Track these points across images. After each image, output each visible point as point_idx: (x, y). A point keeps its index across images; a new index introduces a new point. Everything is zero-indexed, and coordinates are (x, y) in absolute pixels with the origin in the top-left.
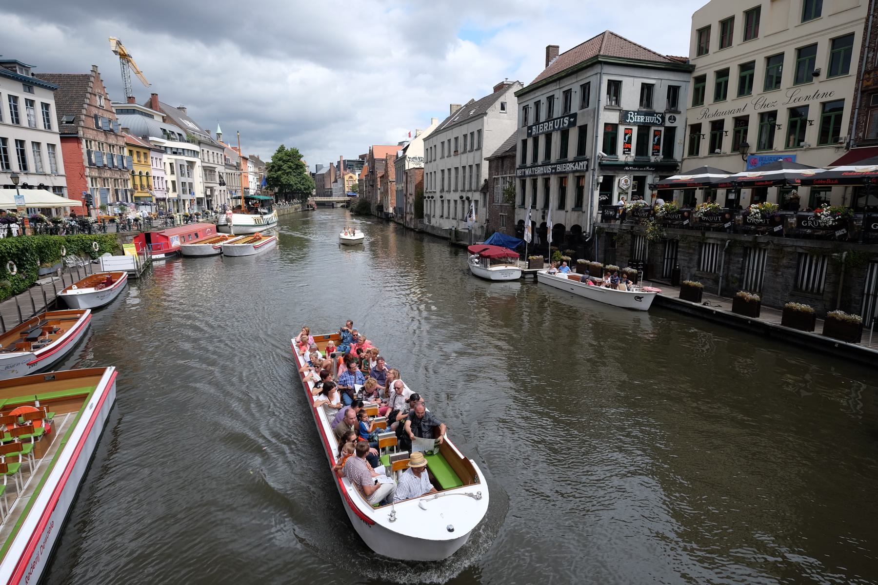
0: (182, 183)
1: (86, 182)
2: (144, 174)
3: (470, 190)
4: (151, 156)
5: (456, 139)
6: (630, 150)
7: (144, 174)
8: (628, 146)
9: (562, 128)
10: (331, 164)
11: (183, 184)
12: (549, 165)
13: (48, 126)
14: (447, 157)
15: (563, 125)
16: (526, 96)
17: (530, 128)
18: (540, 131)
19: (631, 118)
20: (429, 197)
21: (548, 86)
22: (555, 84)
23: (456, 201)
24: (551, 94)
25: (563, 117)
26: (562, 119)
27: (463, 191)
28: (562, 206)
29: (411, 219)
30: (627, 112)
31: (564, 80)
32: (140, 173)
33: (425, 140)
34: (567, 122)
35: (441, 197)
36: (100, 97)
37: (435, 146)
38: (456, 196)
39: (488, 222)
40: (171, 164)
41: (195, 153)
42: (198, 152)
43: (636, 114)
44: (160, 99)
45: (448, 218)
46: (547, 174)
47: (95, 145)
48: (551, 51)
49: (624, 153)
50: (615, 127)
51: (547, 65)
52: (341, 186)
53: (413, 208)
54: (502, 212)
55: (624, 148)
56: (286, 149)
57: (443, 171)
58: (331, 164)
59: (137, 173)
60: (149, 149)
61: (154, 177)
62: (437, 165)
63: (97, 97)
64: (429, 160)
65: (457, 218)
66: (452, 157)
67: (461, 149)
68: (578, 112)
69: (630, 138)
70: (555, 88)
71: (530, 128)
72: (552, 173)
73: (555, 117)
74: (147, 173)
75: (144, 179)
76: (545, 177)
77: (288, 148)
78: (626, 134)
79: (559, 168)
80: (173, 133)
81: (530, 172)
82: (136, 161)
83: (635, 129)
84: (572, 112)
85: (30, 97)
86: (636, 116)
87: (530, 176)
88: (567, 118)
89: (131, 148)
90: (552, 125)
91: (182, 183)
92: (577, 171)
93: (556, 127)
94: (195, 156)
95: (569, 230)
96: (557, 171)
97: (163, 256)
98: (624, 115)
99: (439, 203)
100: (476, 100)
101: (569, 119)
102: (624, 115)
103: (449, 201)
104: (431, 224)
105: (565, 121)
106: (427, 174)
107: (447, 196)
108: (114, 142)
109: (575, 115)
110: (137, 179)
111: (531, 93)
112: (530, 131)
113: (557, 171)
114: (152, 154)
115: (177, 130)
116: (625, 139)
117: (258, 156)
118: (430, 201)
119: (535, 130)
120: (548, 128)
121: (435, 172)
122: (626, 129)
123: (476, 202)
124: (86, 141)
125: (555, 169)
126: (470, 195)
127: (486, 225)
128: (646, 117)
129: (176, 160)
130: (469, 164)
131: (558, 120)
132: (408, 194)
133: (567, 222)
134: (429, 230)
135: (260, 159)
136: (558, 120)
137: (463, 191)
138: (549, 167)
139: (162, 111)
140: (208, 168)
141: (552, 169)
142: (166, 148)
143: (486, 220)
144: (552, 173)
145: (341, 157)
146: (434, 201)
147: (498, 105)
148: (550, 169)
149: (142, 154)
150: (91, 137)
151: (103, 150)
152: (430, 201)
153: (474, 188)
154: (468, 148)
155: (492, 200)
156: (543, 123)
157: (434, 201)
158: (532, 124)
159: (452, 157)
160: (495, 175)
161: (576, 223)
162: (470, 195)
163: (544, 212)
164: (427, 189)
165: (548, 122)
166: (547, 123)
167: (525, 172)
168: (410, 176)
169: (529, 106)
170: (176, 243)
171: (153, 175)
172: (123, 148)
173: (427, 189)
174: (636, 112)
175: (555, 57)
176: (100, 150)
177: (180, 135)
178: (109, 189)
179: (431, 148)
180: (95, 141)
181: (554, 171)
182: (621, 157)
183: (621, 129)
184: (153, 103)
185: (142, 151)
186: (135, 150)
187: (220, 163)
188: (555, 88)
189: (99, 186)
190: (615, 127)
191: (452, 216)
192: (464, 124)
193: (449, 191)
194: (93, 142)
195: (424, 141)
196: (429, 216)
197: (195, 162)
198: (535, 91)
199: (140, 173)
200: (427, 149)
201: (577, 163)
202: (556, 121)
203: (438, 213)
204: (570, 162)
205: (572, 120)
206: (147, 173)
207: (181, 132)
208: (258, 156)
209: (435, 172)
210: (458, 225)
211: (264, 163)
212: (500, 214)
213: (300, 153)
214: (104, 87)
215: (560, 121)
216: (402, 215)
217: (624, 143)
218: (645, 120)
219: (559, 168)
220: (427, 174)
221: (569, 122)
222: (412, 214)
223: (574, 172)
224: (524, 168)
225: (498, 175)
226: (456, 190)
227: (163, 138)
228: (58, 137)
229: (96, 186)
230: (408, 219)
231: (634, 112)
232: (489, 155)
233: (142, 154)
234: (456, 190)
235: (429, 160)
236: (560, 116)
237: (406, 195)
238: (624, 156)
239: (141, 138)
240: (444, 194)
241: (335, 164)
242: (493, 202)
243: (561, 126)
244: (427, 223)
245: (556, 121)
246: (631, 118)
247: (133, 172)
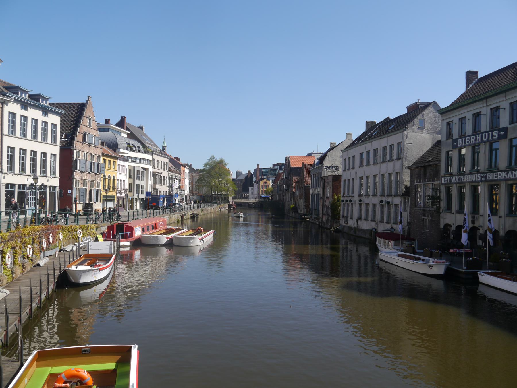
0: (137, 185)
1: (72, 183)
2: (112, 177)
3: (390, 195)
4: (118, 163)
5: (376, 151)
7: (112, 177)
9: (491, 141)
10: (249, 171)
11: (138, 186)
12: (478, 174)
13: (54, 141)
14: (366, 166)
15: (492, 137)
16: (450, 113)
17: (456, 141)
18: (467, 143)
20: (347, 201)
21: (474, 104)
22: (481, 102)
23: (374, 205)
24: (477, 111)
25: (493, 131)
26: (490, 133)
27: (382, 195)
28: (494, 212)
29: (328, 219)
31: (492, 98)
32: (109, 176)
33: (343, 151)
34: (496, 135)
35: (360, 201)
36: (90, 119)
38: (376, 200)
39: (410, 225)
40: (130, 170)
41: (149, 161)
42: (150, 161)
44: (127, 121)
45: (366, 219)
46: (475, 182)
47: (82, 154)
48: (471, 75)
51: (467, 86)
52: (257, 189)
53: (330, 209)
54: (424, 216)
56: (215, 158)
57: (361, 178)
58: (249, 171)
59: (107, 177)
60: (117, 158)
61: (118, 180)
62: (356, 173)
63: (88, 119)
64: (347, 168)
65: (376, 220)
66: (372, 165)
67: (379, 159)
68: (509, 126)
70: (481, 106)
71: (456, 141)
72: (481, 181)
73: (483, 130)
74: (114, 177)
75: (112, 181)
76: (473, 184)
77: (217, 158)
79: (490, 177)
80: (134, 146)
81: (457, 180)
82: (107, 168)
84: (502, 126)
85: (45, 119)
87: (457, 183)
88: (497, 132)
89: (105, 158)
90: (480, 138)
91: (137, 185)
92: (510, 179)
94: (148, 164)
95: (504, 235)
96: (488, 179)
97: (128, 243)
99: (356, 208)
100: (392, 117)
101: (499, 132)
103: (367, 205)
104: (348, 225)
105: (494, 134)
106: (345, 180)
107: (366, 200)
108: (94, 153)
109: (505, 129)
110: (107, 180)
111: (455, 111)
112: (455, 143)
113: (488, 179)
114: (119, 162)
115: (137, 144)
117: (191, 165)
118: (348, 205)
119: (461, 142)
120: (475, 140)
121: (353, 179)
123: (396, 206)
124: (77, 152)
125: (486, 177)
126: (390, 199)
127: (407, 227)
129: (134, 167)
130: (388, 172)
131: (487, 134)
132: (325, 198)
133: (501, 227)
134: (346, 230)
135: (192, 166)
136: (487, 134)
137: (382, 195)
138: (479, 176)
139: (128, 129)
140: (157, 174)
141: (482, 177)
142: (128, 157)
143: (408, 222)
144: (481, 181)
145: (258, 165)
146: (352, 204)
147: (416, 121)
148: (479, 177)
149: (112, 162)
150: (80, 149)
151: (86, 159)
152: (348, 205)
153: (393, 193)
154: (388, 158)
155: (414, 204)
156: (470, 136)
157: (352, 204)
158: (457, 137)
159: (372, 165)
160: (417, 182)
161: (511, 229)
162: (390, 199)
163: (474, 217)
164: (344, 193)
165: (475, 135)
166: (474, 137)
167: (450, 180)
168: (328, 182)
169: (454, 122)
170: (138, 233)
171: (118, 178)
172: (100, 157)
173: (344, 193)
176: (84, 158)
177: (139, 147)
178: (86, 188)
179: (349, 158)
180: (82, 151)
181: (483, 179)
184: (121, 123)
185: (112, 160)
186: (107, 159)
187: (165, 170)
188: (481, 106)
189: (80, 187)
191: (370, 218)
192: (384, 138)
193: (367, 195)
194: (81, 152)
195: (342, 152)
196: (346, 218)
197: (148, 169)
198: (460, 109)
199: (109, 176)
200: (345, 159)
201: (510, 173)
202: (484, 134)
203: (356, 214)
204: (502, 171)
205: (502, 133)
206: (114, 177)
207: (140, 145)
208: (191, 165)
209: (353, 179)
210: (377, 227)
211: (194, 170)
212: (423, 217)
213: (226, 161)
214: (93, 112)
215: (489, 135)
216: (318, 215)
219: (490, 177)
220: (345, 180)
221: (499, 136)
222: (328, 215)
223: (506, 180)
224: (450, 176)
225: (420, 182)
226: (374, 195)
227: (127, 149)
228: (58, 149)
229: (78, 186)
230: (324, 219)
232: (410, 164)
233: (112, 162)
234: (374, 195)
235: (347, 168)
236: (488, 129)
237: (323, 199)
239: (112, 149)
240: (362, 198)
241: (252, 172)
242: (416, 207)
243: (490, 138)
244: (345, 224)
245: (484, 134)
247: (104, 176)
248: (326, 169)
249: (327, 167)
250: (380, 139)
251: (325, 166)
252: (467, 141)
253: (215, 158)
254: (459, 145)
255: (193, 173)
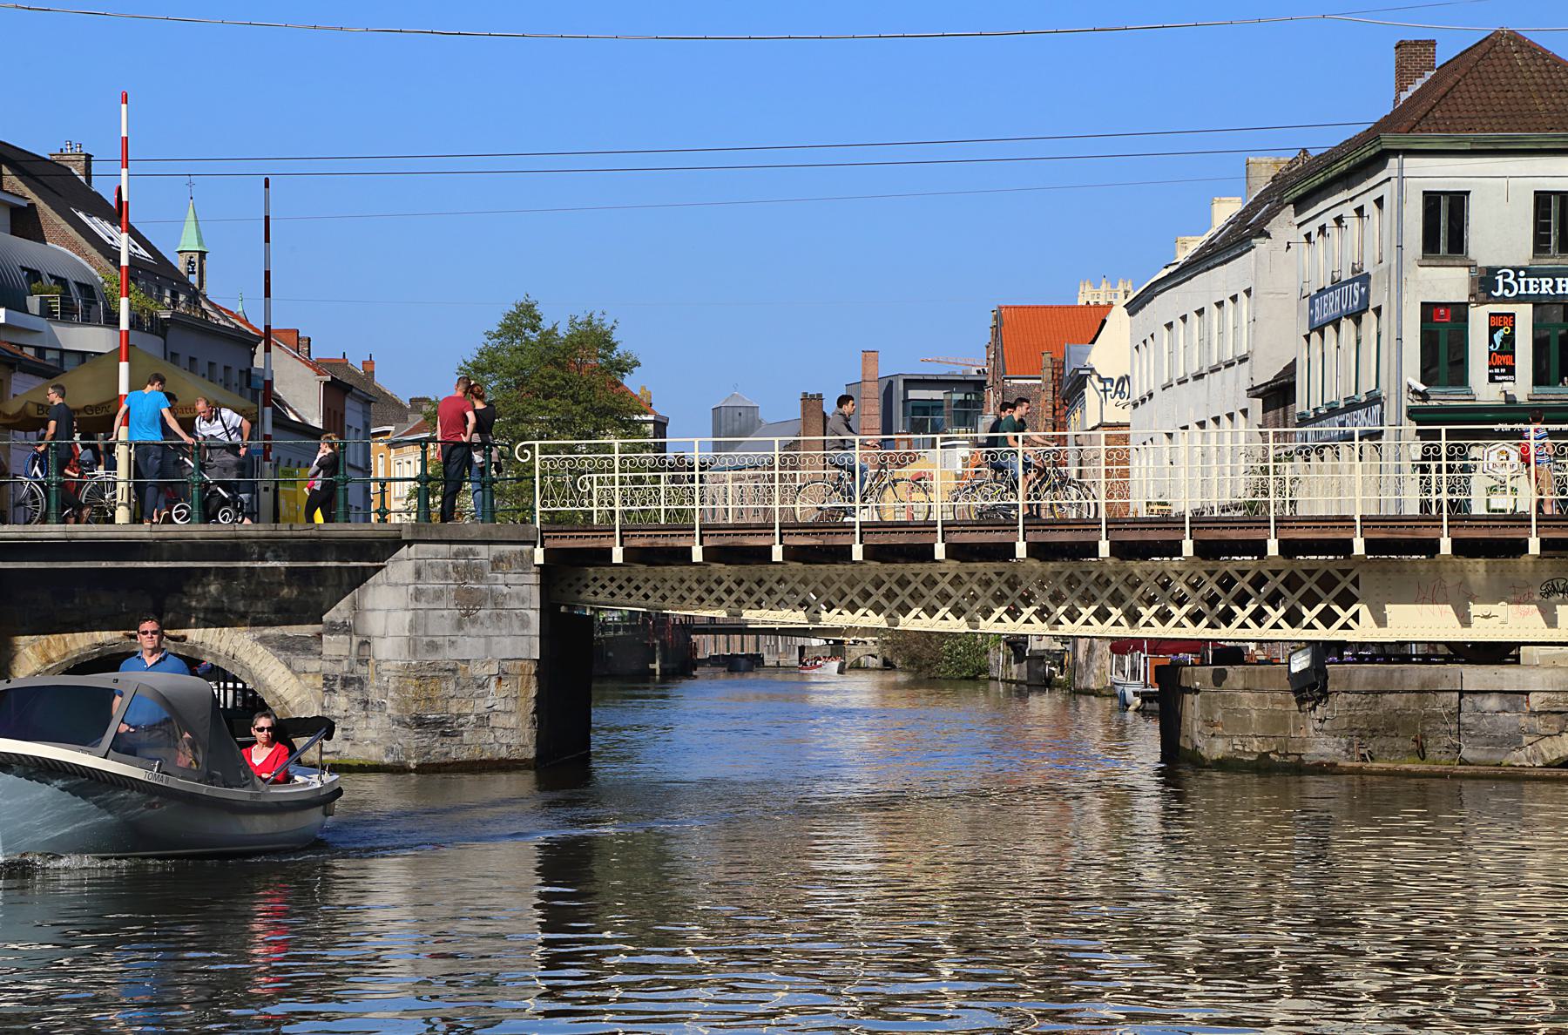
6: (1511, 371)
8: (1506, 359)
19: (1507, 286)
30: (1493, 271)
34: (1356, 293)
37: (1152, 336)
43: (1522, 273)
48: (1412, 54)
49: (1492, 379)
50: (1459, 312)
55: (1491, 367)
56: (546, 325)
69: (1509, 340)
77: (558, 318)
78: (1493, 330)
83: (1524, 314)
86: (1522, 281)
90: (1338, 299)
93: (1344, 307)
98: (1485, 283)
102: (1485, 283)
116: (1491, 341)
122: (1491, 315)
128: (1559, 280)
174: (1525, 269)
175: (1422, 75)
182: (1484, 390)
183: (1479, 318)
190: (1459, 312)
208: (369, 364)
211: (398, 405)
217: (1490, 353)
218: (1554, 288)
231: (1516, 270)
238: (1496, 387)
246: (1507, 286)
248: (1105, 391)
249: (1112, 380)
250: (1209, 269)
251: (1100, 379)
252: (1326, 305)
253: (546, 325)
254: (1317, 319)
255: (391, 428)
